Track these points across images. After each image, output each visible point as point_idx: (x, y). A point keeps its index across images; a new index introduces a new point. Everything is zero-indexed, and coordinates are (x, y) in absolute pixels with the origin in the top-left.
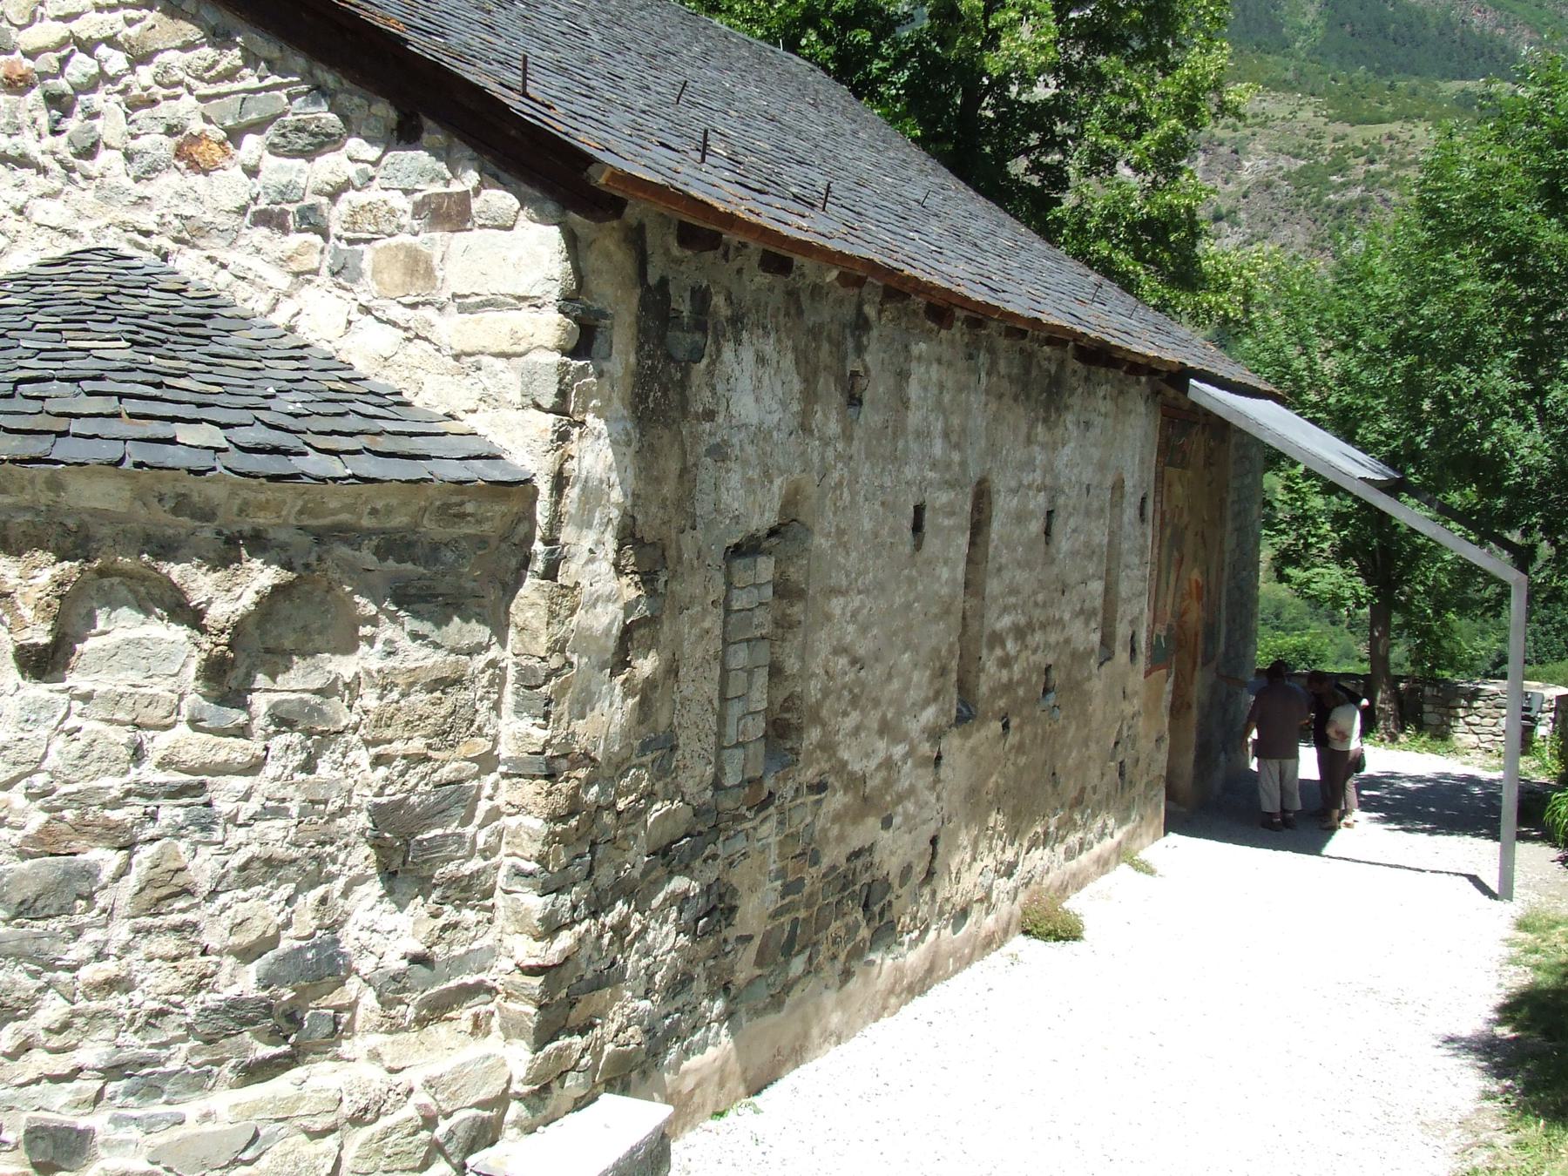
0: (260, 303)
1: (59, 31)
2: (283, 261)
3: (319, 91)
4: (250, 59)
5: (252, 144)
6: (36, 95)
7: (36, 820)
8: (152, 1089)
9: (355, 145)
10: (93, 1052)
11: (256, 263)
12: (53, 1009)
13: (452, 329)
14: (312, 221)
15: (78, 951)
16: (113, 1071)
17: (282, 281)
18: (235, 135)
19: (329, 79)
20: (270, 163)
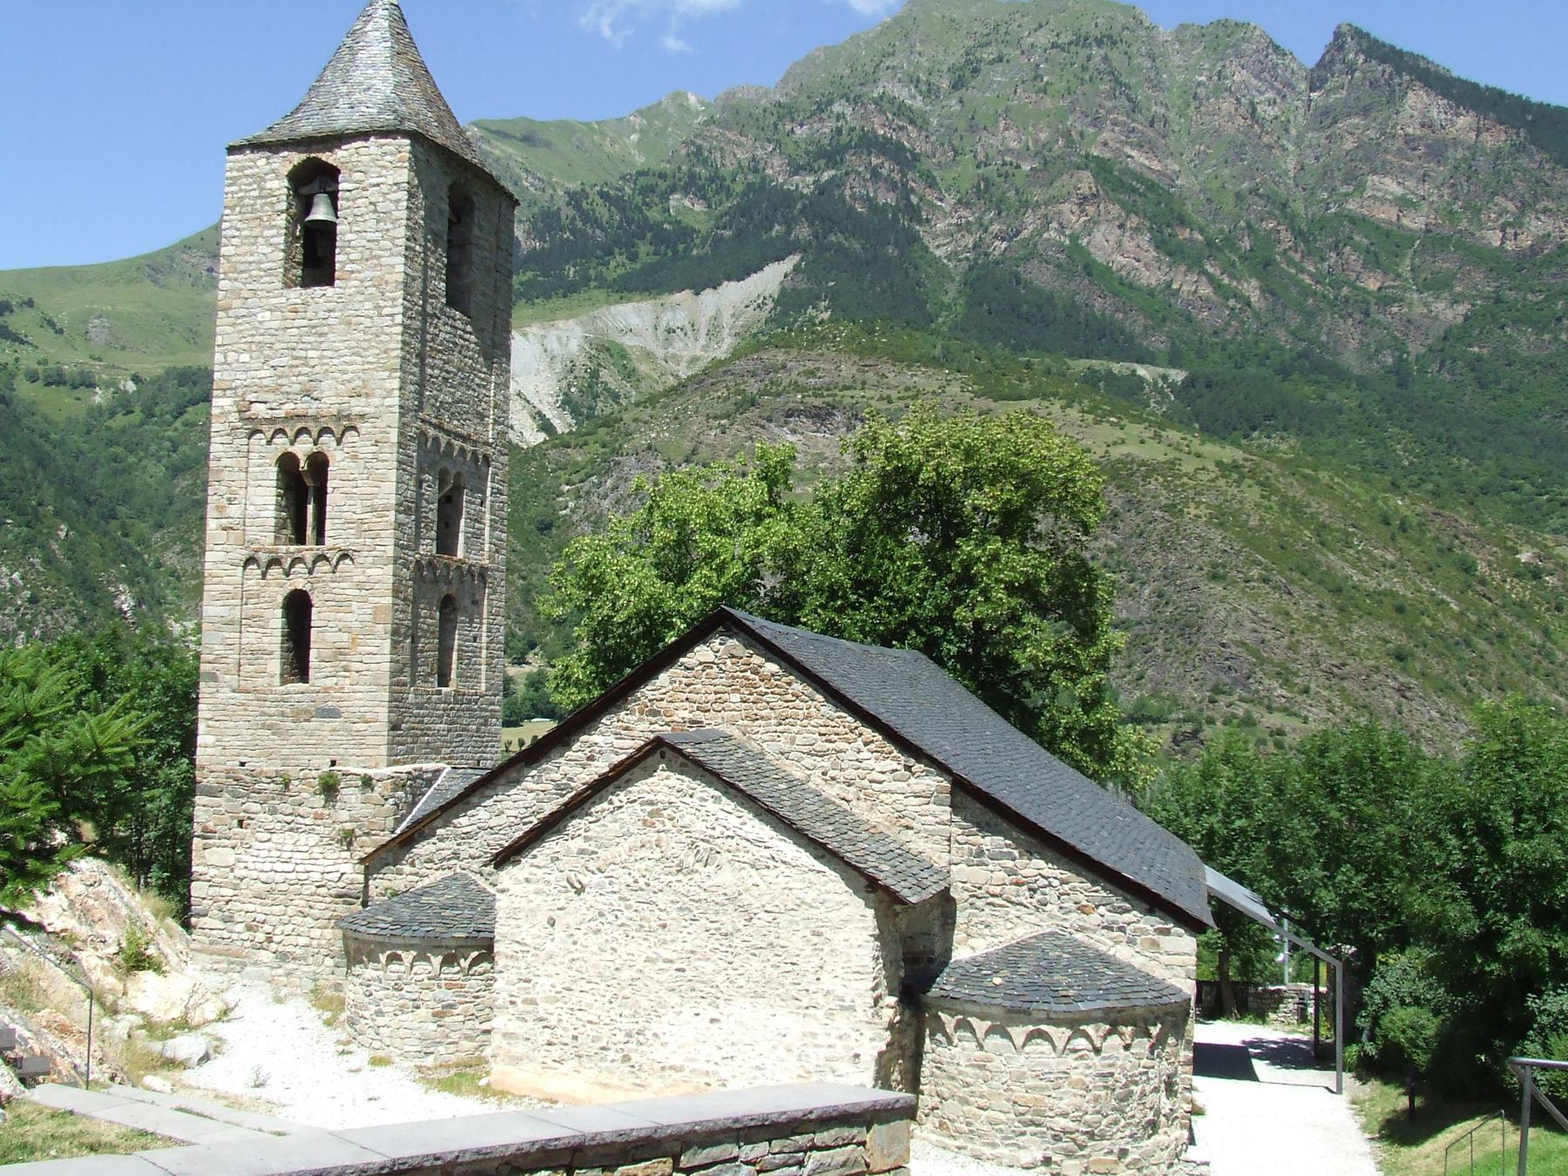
0: (1103, 948)
1: (1036, 872)
2: (1111, 939)
3: (1126, 900)
4: (1104, 889)
5: (1102, 910)
6: (1025, 887)
7: (1124, 1081)
8: (1136, 1140)
9: (1135, 912)
10: (1128, 1132)
11: (1102, 938)
12: (1123, 1122)
13: (1164, 958)
14: (1122, 929)
15: (1128, 1109)
16: (1130, 1137)
17: (1112, 943)
18: (1097, 907)
19: (1129, 897)
20: (1108, 914)
